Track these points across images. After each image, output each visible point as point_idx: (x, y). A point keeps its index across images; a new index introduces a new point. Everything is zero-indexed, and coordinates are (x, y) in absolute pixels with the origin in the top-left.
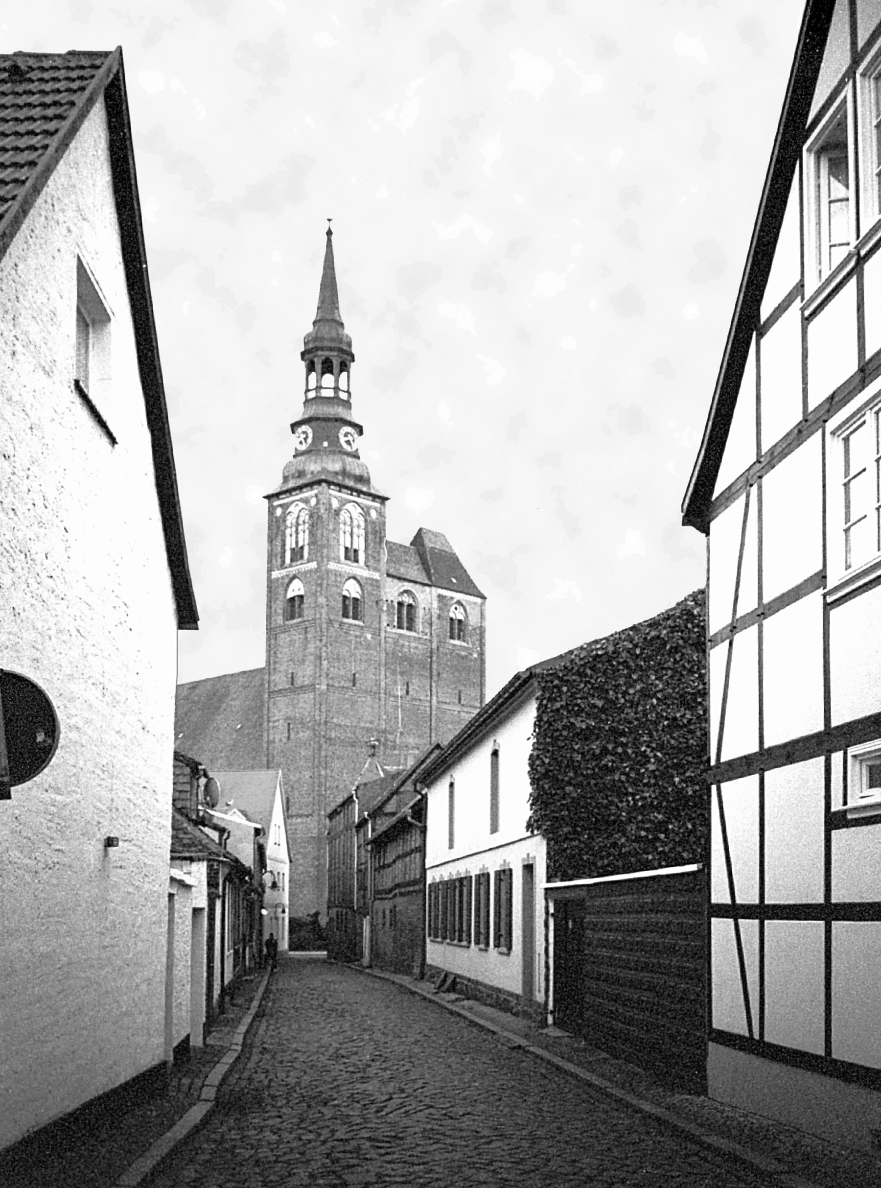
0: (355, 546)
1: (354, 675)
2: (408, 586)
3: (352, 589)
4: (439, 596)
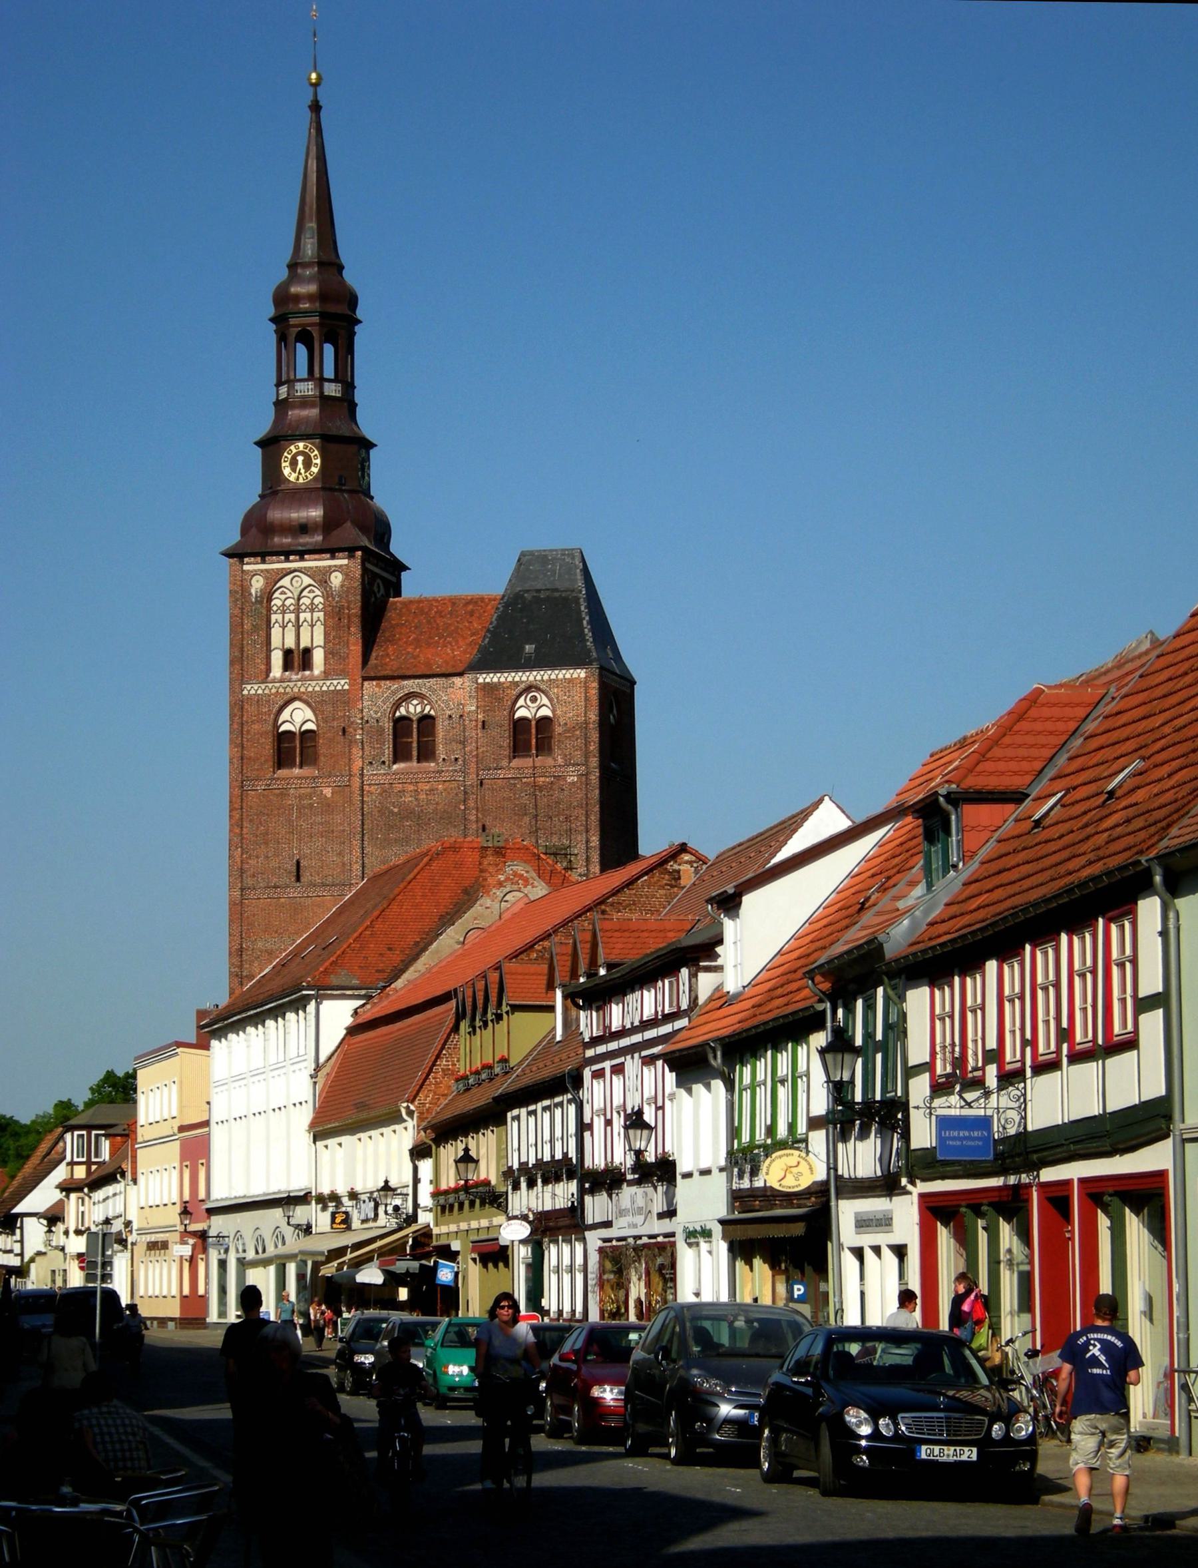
1: (298, 863)
2: (410, 685)
3: (298, 718)
4: (486, 685)
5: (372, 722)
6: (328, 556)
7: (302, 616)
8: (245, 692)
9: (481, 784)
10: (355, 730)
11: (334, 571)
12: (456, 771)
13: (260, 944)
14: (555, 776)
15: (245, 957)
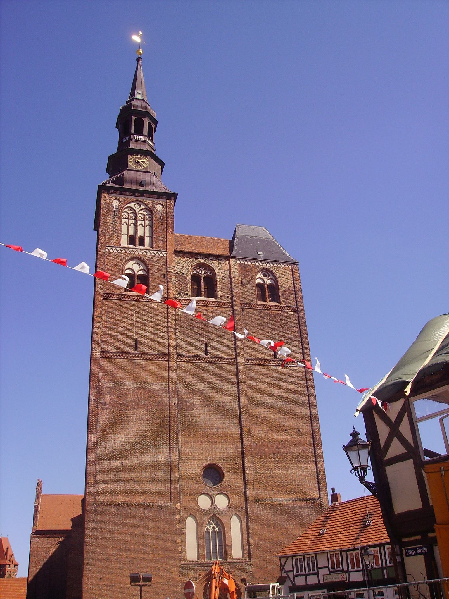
0: (140, 233)
1: (136, 341)
4: (240, 265)
5: (180, 274)
6: (156, 196)
7: (139, 222)
8: (107, 250)
9: (243, 311)
10: (171, 276)
11: (158, 204)
12: (228, 303)
13: (111, 385)
14: (282, 311)
15: (100, 391)
